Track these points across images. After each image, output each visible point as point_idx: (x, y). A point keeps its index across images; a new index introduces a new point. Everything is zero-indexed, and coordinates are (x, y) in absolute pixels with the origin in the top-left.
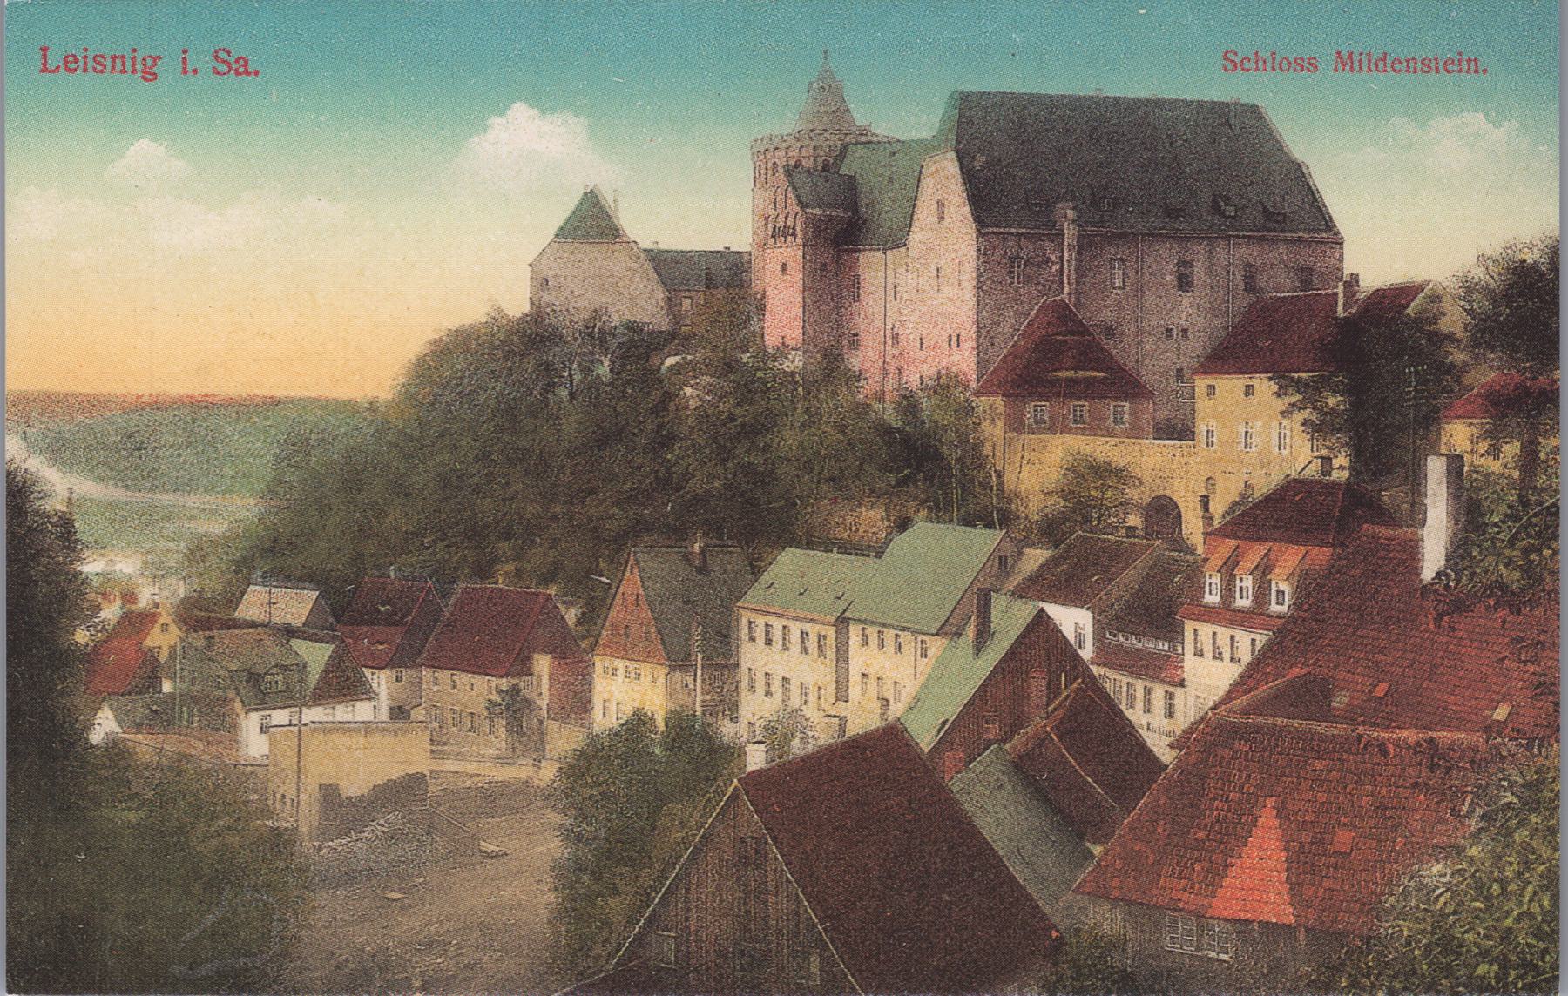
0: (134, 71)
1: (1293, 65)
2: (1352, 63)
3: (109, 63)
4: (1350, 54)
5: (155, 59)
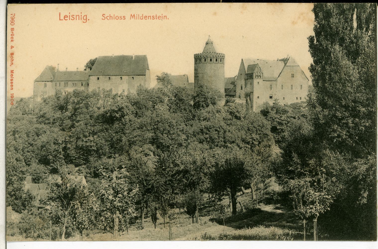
1: (119, 18)
3: (75, 17)
4: (134, 15)
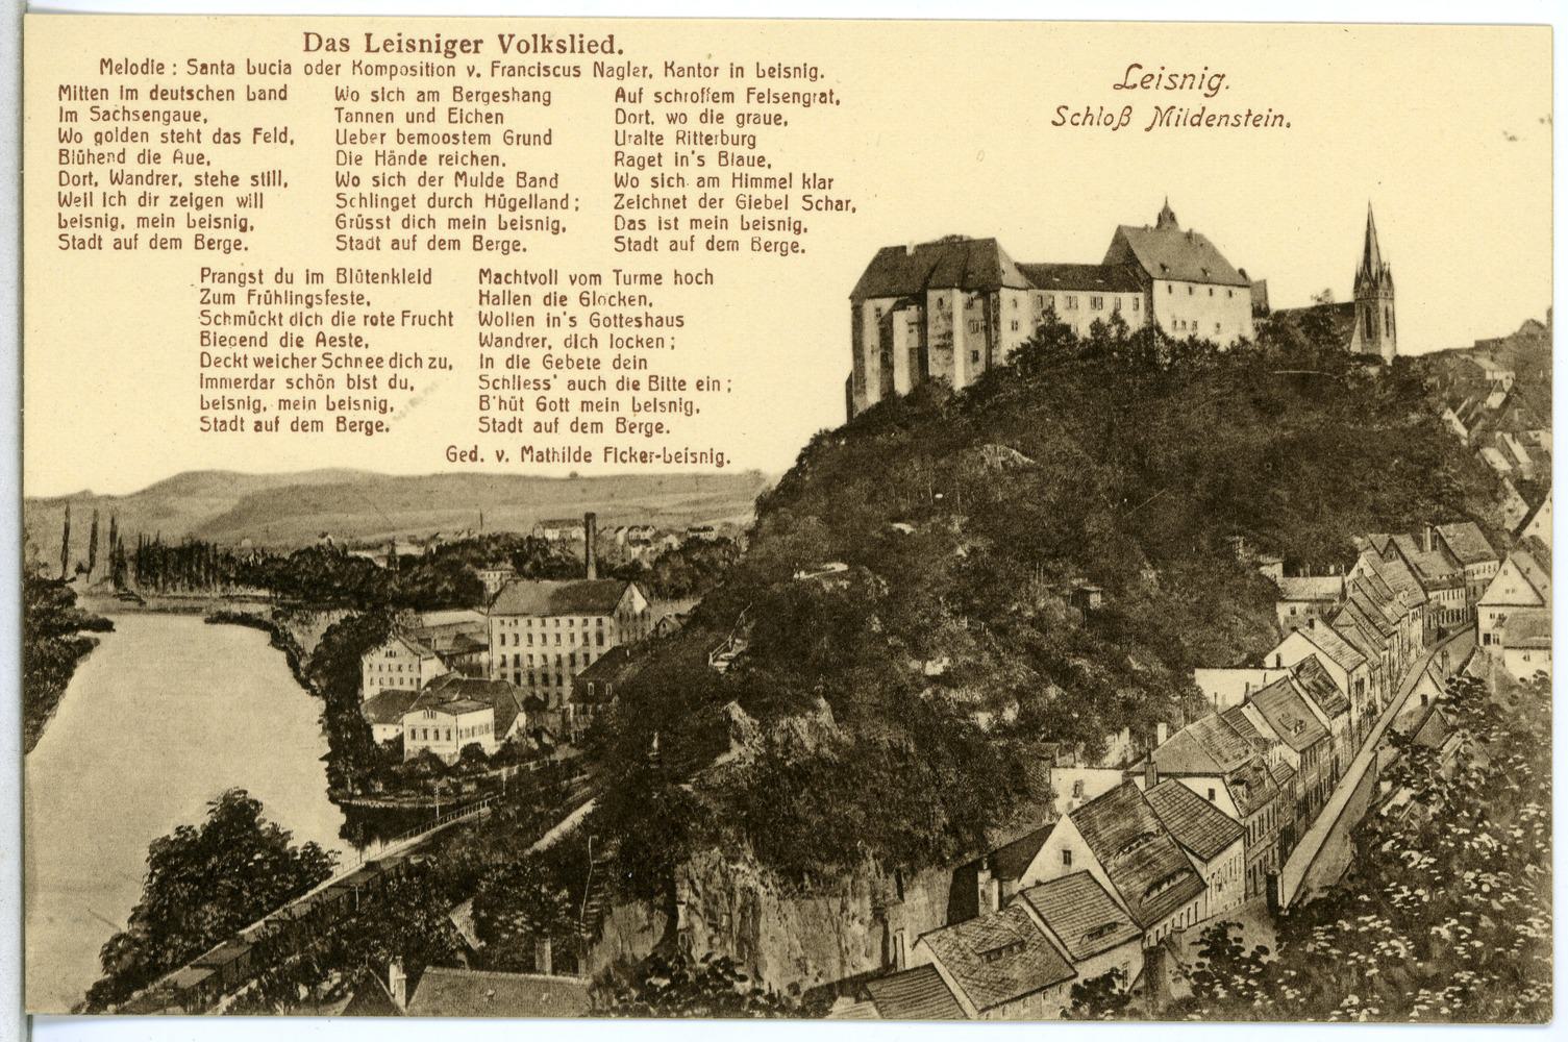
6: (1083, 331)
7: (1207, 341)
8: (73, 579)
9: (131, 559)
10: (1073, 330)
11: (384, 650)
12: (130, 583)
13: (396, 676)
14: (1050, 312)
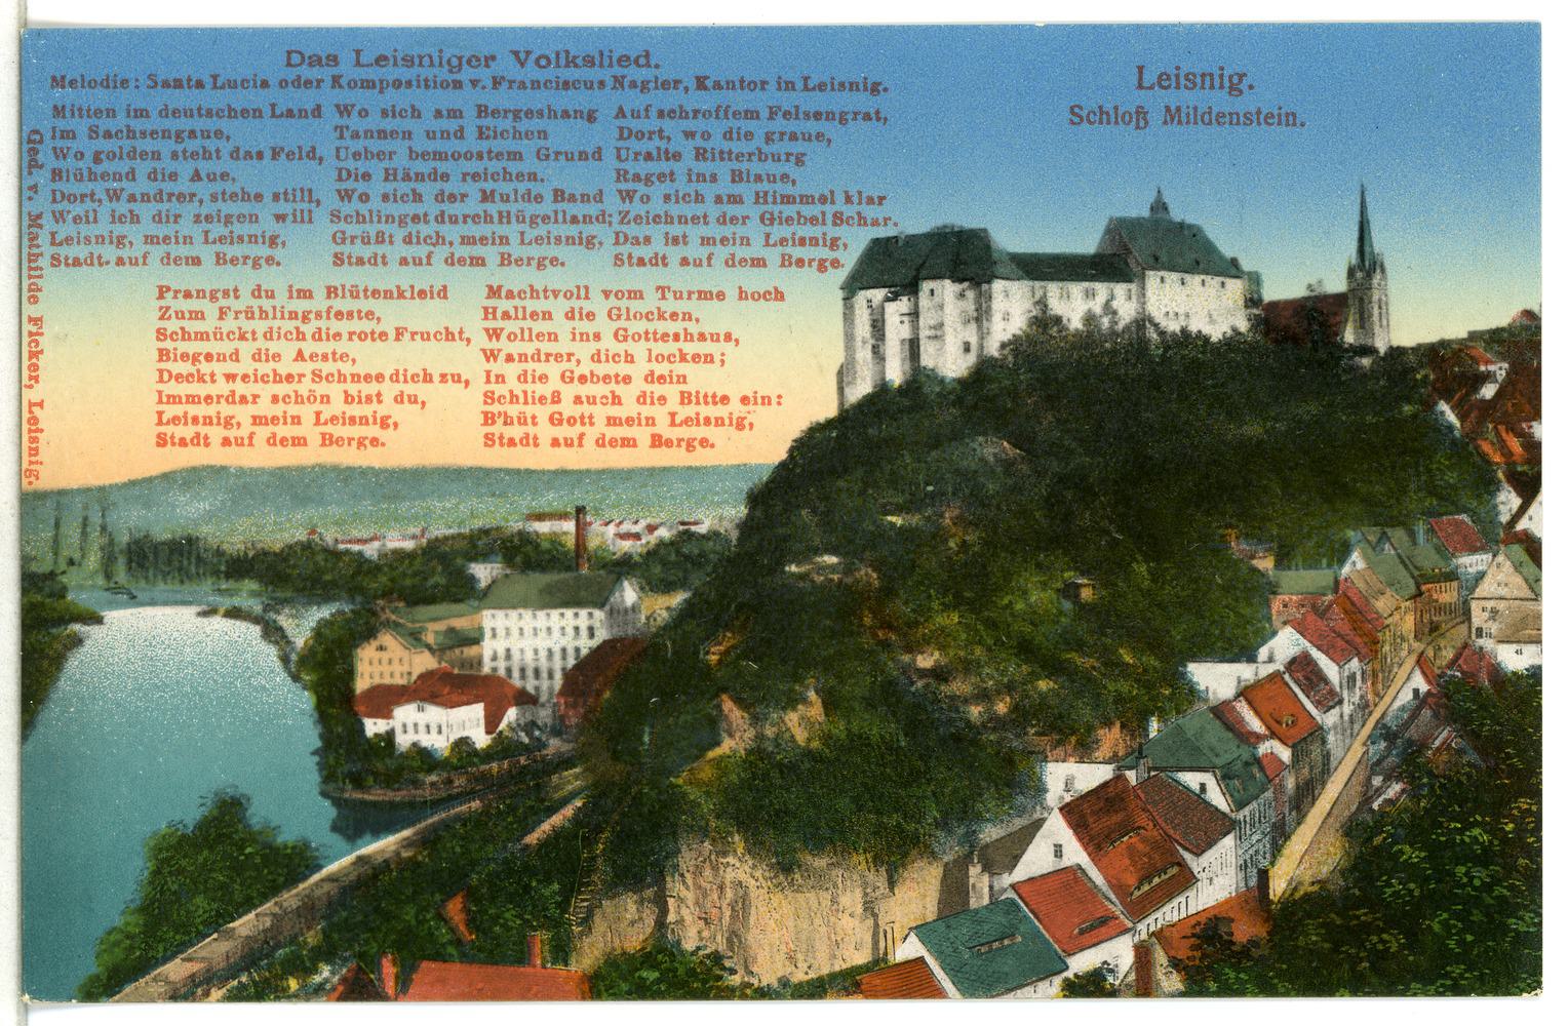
0: (1222, 87)
2: (1180, 117)
3: (1198, 80)
4: (1178, 109)
5: (1241, 76)
6: (1076, 323)
7: (1200, 332)
8: (64, 573)
9: (121, 551)
10: (1065, 321)
11: (374, 644)
12: (121, 575)
13: (386, 669)
14: (1042, 303)
